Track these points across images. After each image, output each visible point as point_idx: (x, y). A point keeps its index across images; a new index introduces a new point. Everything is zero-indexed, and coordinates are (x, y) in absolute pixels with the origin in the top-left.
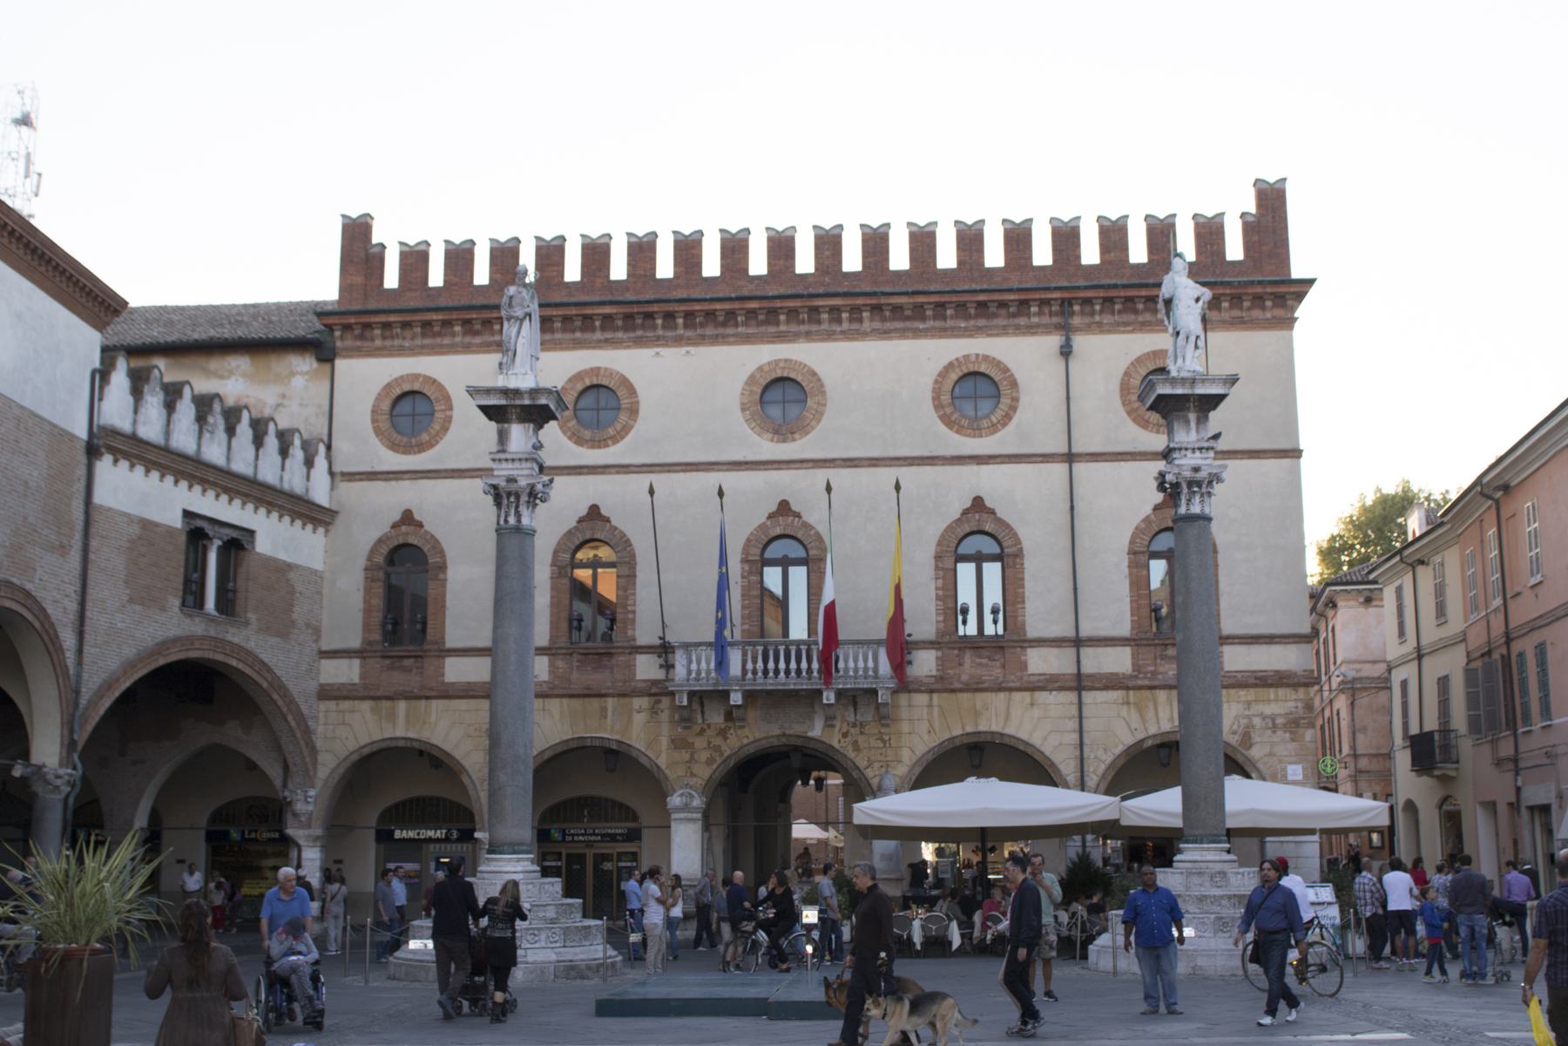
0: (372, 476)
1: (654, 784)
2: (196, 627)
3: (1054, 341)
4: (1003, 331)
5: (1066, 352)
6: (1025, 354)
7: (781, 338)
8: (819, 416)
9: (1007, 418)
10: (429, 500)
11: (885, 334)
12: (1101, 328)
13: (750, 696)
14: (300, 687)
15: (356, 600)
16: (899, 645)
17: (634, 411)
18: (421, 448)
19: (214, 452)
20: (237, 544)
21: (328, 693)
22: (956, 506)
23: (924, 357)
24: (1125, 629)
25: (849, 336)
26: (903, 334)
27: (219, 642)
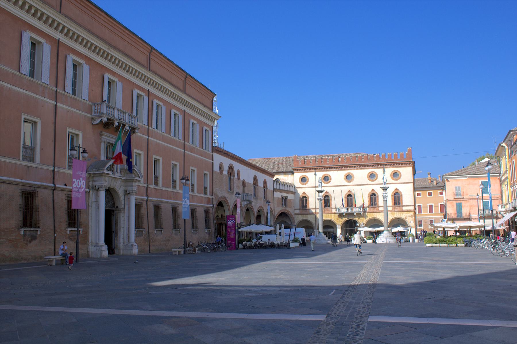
0: (299, 188)
1: (335, 225)
2: (283, 208)
3: (382, 169)
4: (376, 168)
5: (384, 171)
6: (379, 171)
7: (348, 170)
8: (353, 179)
9: (376, 179)
10: (307, 191)
11: (361, 169)
12: (388, 168)
13: (346, 214)
14: (293, 214)
15: (299, 203)
16: (364, 208)
17: (331, 179)
18: (305, 184)
19: (283, 189)
20: (286, 198)
21: (296, 214)
22: (370, 190)
23: (366, 172)
24: (391, 205)
25: (356, 169)
26: (363, 169)
27: (285, 210)
